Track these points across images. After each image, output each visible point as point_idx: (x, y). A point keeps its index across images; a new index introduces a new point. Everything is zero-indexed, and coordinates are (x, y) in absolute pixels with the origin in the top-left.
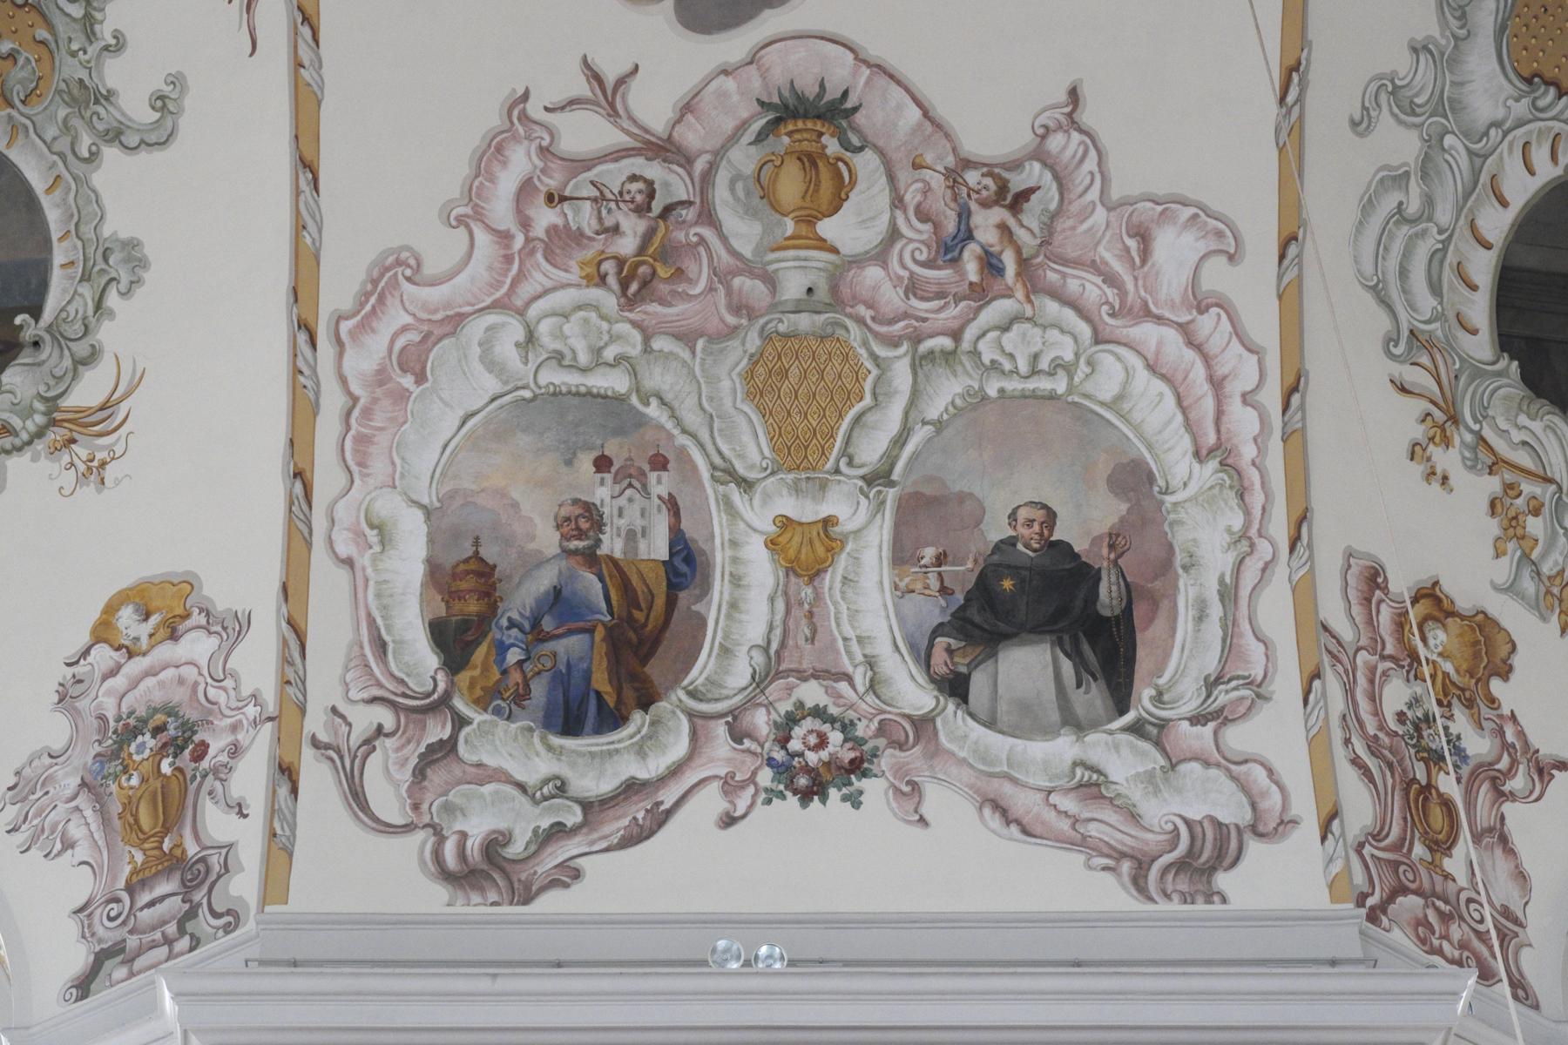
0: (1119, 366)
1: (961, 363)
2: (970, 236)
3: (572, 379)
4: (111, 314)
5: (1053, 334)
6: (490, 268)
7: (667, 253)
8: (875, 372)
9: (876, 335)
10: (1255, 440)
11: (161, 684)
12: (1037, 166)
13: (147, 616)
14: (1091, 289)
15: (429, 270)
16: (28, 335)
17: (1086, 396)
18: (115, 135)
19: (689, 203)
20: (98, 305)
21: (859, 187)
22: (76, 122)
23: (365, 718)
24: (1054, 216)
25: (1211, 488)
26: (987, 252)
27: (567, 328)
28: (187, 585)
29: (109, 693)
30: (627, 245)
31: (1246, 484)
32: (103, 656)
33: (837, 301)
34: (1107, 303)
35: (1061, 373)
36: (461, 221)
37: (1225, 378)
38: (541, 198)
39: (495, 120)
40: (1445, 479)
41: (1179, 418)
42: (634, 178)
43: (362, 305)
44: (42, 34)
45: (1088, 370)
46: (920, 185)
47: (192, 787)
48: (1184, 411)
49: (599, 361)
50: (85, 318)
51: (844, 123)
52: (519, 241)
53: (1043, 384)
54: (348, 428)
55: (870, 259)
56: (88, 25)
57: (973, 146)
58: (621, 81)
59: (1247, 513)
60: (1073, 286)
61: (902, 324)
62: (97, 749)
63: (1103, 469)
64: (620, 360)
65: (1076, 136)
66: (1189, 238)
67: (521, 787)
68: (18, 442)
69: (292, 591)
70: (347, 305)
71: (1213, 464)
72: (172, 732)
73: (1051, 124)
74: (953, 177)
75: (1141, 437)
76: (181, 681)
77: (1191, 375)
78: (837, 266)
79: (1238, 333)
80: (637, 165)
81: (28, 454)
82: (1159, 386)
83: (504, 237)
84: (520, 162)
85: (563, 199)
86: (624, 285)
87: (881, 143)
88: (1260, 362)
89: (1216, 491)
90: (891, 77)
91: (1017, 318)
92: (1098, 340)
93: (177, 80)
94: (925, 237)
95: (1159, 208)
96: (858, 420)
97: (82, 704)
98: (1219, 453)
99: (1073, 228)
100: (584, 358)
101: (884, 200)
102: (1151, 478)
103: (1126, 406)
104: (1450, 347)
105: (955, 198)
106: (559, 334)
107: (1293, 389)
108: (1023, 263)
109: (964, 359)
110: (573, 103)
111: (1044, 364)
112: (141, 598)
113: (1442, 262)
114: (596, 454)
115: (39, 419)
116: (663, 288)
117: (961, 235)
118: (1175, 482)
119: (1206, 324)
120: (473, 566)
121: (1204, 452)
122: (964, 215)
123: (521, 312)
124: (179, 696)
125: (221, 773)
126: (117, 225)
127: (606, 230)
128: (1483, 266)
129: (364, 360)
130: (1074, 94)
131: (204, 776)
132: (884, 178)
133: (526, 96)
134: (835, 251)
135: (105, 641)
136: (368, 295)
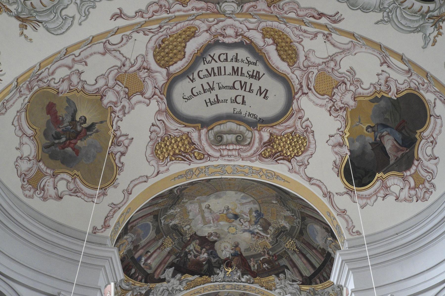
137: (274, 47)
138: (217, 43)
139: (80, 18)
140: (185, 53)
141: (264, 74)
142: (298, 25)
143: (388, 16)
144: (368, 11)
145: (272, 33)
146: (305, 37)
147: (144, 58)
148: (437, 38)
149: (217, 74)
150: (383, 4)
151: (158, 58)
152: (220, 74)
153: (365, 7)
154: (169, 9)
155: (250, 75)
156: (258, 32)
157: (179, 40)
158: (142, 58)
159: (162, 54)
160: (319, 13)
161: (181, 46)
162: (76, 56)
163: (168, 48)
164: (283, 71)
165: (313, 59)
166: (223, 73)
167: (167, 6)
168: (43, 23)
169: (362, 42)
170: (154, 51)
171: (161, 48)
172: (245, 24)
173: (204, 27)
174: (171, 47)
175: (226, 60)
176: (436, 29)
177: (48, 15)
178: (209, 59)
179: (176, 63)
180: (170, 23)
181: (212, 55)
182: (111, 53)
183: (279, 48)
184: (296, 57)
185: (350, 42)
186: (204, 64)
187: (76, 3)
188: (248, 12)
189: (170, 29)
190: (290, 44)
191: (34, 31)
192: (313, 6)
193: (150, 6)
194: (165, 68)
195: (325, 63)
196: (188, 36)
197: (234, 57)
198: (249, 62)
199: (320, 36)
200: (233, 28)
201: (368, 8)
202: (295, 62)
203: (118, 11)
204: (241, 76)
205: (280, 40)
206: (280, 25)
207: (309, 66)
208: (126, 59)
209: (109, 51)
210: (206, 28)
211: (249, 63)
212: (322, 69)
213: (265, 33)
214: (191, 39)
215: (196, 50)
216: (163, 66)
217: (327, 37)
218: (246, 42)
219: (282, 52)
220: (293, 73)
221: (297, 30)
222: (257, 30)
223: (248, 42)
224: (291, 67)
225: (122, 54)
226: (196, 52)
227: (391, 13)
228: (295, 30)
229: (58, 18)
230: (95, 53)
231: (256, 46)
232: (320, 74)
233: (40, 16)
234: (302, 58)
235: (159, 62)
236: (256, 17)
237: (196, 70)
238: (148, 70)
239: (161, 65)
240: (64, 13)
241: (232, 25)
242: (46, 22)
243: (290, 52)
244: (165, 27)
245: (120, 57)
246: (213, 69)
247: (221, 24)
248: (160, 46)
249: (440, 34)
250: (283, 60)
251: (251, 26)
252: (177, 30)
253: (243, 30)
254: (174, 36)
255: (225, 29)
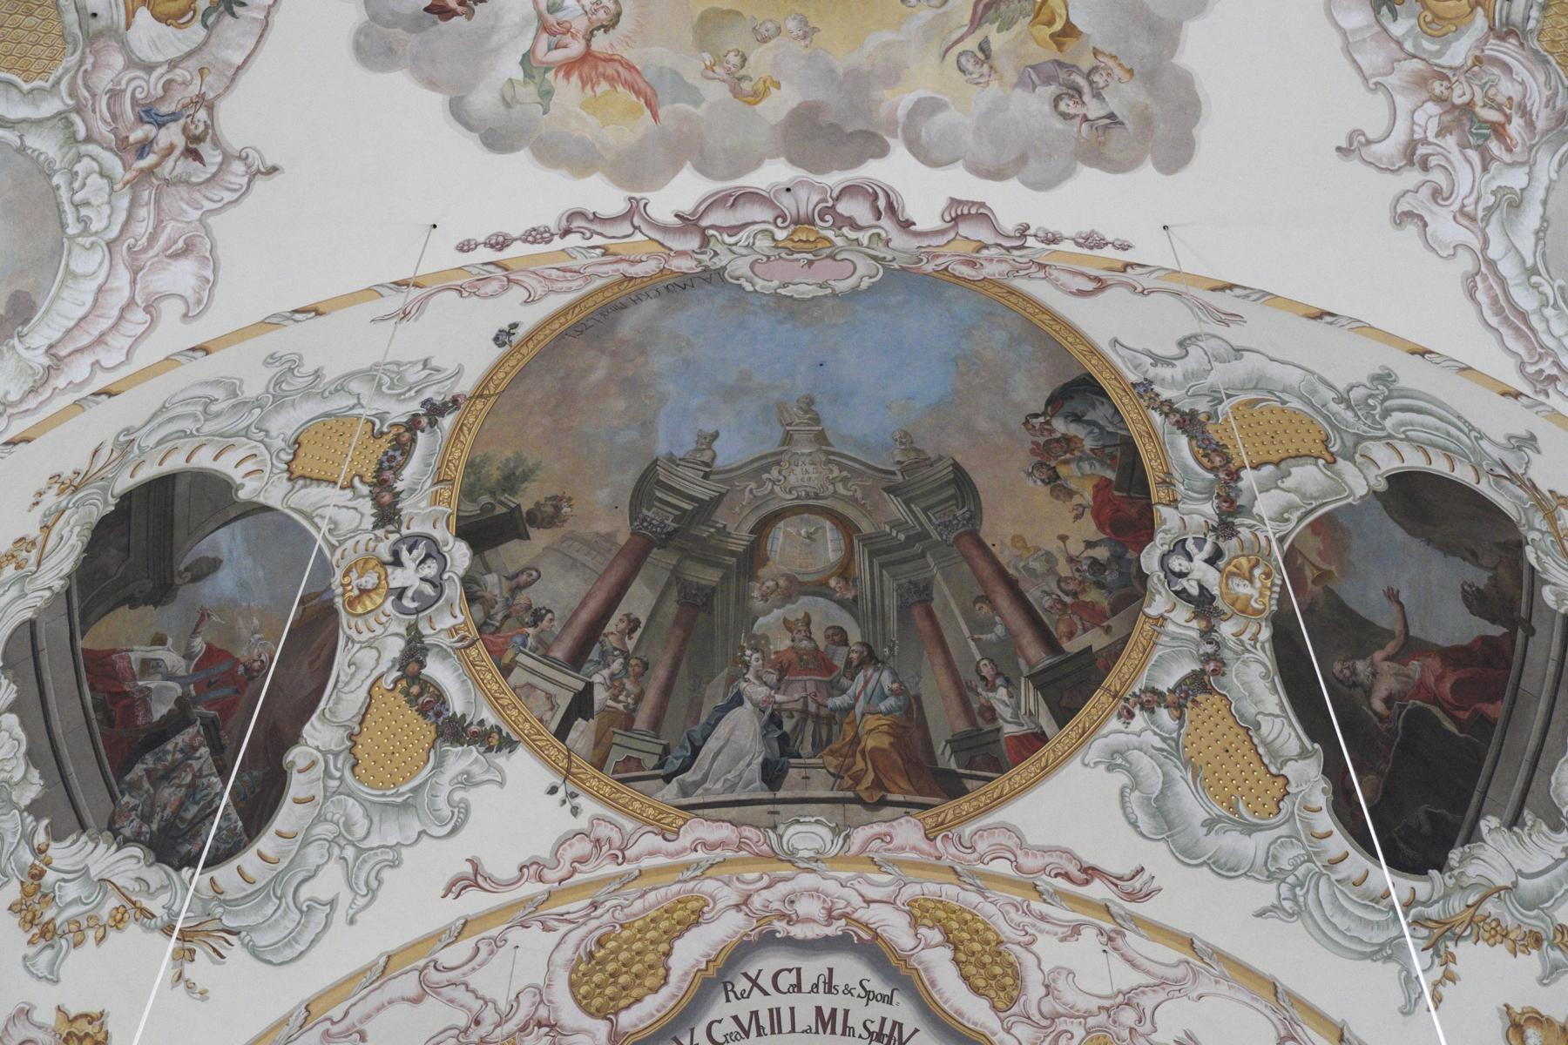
0: (95, 267)
1: (70, 149)
2: (160, 126)
5: (106, 210)
8: (47, 85)
9: (74, 78)
10: (71, 383)
12: (219, 159)
14: (142, 228)
17: (70, 251)
21: (179, 33)
24: (187, 183)
25: (31, 368)
26: (152, 142)
31: (41, 390)
33: (92, 39)
34: (137, 241)
35: (81, 226)
37: (106, 344)
40: (37, 504)
41: (71, 324)
45: (87, 245)
46: (189, 78)
48: (77, 324)
51: (222, 9)
53: (70, 216)
55: (129, 56)
57: (224, 109)
59: (21, 401)
60: (142, 212)
61: (87, 94)
63: (23, 285)
65: (246, 179)
66: (192, 281)
71: (46, 361)
73: (250, 160)
74: (200, 101)
75: (53, 302)
77: (101, 320)
78: (116, 31)
79: (138, 340)
82: (89, 299)
87: (213, 40)
88: (122, 364)
89: (30, 372)
90: (261, 36)
91: (111, 181)
92: (110, 245)
94: (153, 92)
95: (208, 254)
96: (11, 84)
98: (56, 360)
99: (182, 199)
101: (173, 53)
102: (26, 322)
103: (70, 282)
104: (122, 466)
105: (185, 107)
107: (108, 393)
108: (150, 171)
109: (74, 150)
111: (84, 212)
113: (179, 438)
117: (159, 119)
118: (28, 340)
119: (139, 315)
121: (53, 351)
122: (174, 116)
128: (175, 463)
130: (274, 170)
132: (187, 49)
134: (128, 26)
137: (947, 953)
138: (768, 940)
139: (353, 902)
140: (668, 970)
141: (916, 1031)
142: (1019, 899)
143: (1294, 898)
144: (1233, 874)
145: (941, 914)
146: (1041, 931)
147: (541, 995)
148: (1441, 988)
149: (768, 1030)
150: (1275, 858)
151: (584, 990)
152: (776, 1028)
153: (1222, 861)
154: (622, 851)
155: (871, 1034)
156: (898, 909)
157: (651, 935)
158: (535, 995)
159: (597, 978)
160: (1085, 866)
161: (655, 951)
162: (333, 1023)
163: (616, 959)
164: (976, 1024)
165: (1069, 995)
166: (786, 1026)
167: (617, 842)
168: (244, 934)
169: (1218, 969)
170: (574, 970)
171: (593, 962)
172: (857, 886)
173: (729, 895)
174: (623, 956)
175: (797, 987)
176: (1437, 961)
177: (259, 907)
178: (742, 984)
179: (638, 1000)
180: (622, 891)
181: (753, 974)
182: (439, 994)
183: (962, 957)
184: (1015, 986)
185: (1181, 962)
186: (728, 1000)
187: (344, 858)
188: (865, 855)
189: (622, 908)
190: (997, 947)
191: (214, 962)
192: (1064, 844)
193: (566, 846)
194: (605, 1018)
195: (1107, 1009)
196: (678, 923)
197: (822, 979)
198: (868, 993)
199: (1088, 934)
200: (819, 897)
201: (1231, 864)
202: (1013, 1001)
203: (468, 869)
204: (844, 1034)
205: (966, 936)
206: (963, 894)
207: (1060, 1015)
208: (486, 1003)
209: (436, 989)
210: (735, 899)
211: (869, 996)
212: (1099, 1028)
213: (918, 914)
214: (687, 929)
215: (704, 960)
216: (600, 1013)
217: (1110, 939)
218: (859, 937)
219: (971, 970)
220: (1008, 1031)
221: (1018, 910)
222: (894, 903)
223: (865, 936)
224: (1001, 1014)
225: (473, 992)
226: (703, 966)
227: (1302, 886)
228: (1012, 910)
229: (285, 913)
230: (390, 1002)
231: (892, 949)
232: (1092, 1040)
233: (236, 914)
234: (1034, 991)
235: (584, 1002)
236: (889, 869)
237: (699, 1020)
238: (552, 1027)
239: (593, 1010)
240: (305, 893)
241: (817, 890)
242: (250, 929)
243: (998, 970)
244: (608, 904)
245: (469, 999)
246: (755, 1014)
247: (782, 889)
248: (591, 955)
249: (1449, 977)
250: (976, 990)
251: (872, 893)
252: (645, 910)
253: (849, 904)
254: (636, 924)
255: (792, 902)
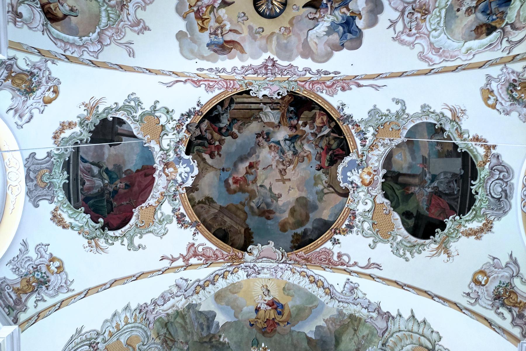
3: (443, 20)
4: (434, 110)
6: (422, 39)
7: (421, 8)
11: (502, 93)
13: (489, 98)
15: (421, 50)
16: (439, 126)
18: (404, 111)
19: (412, 5)
20: (433, 113)
22: (402, 118)
23: (505, 44)
27: (433, 23)
28: (482, 89)
29: (506, 104)
30: (419, 15)
32: (498, 106)
36: (413, 46)
38: (410, 32)
39: (397, 42)
42: (408, 16)
43: (427, 61)
44: (388, 123)
47: (522, 81)
49: (440, 16)
50: (435, 115)
52: (417, 35)
54: (449, 60)
56: (386, 116)
58: (391, 22)
62: (517, 105)
64: (440, 12)
67: (522, 6)
68: (459, 127)
69: (481, 66)
70: (427, 64)
72: (511, 88)
76: (501, 88)
80: (405, 16)
81: (461, 125)
83: (417, 38)
84: (404, 37)
85: (410, 28)
86: (426, 14)
93: (393, 100)
97: (508, 110)
100: (439, 19)
106: (434, 24)
110: (394, 29)
112: (486, 99)
114: (456, 12)
115: (454, 123)
116: (427, 7)
120: (476, 31)
123: (430, 32)
124: (504, 88)
125: (518, 75)
126: (419, 110)
127: (416, 20)
129: (436, 59)
131: (519, 79)
133: (393, 38)
135: (495, 106)
136: (425, 61)
